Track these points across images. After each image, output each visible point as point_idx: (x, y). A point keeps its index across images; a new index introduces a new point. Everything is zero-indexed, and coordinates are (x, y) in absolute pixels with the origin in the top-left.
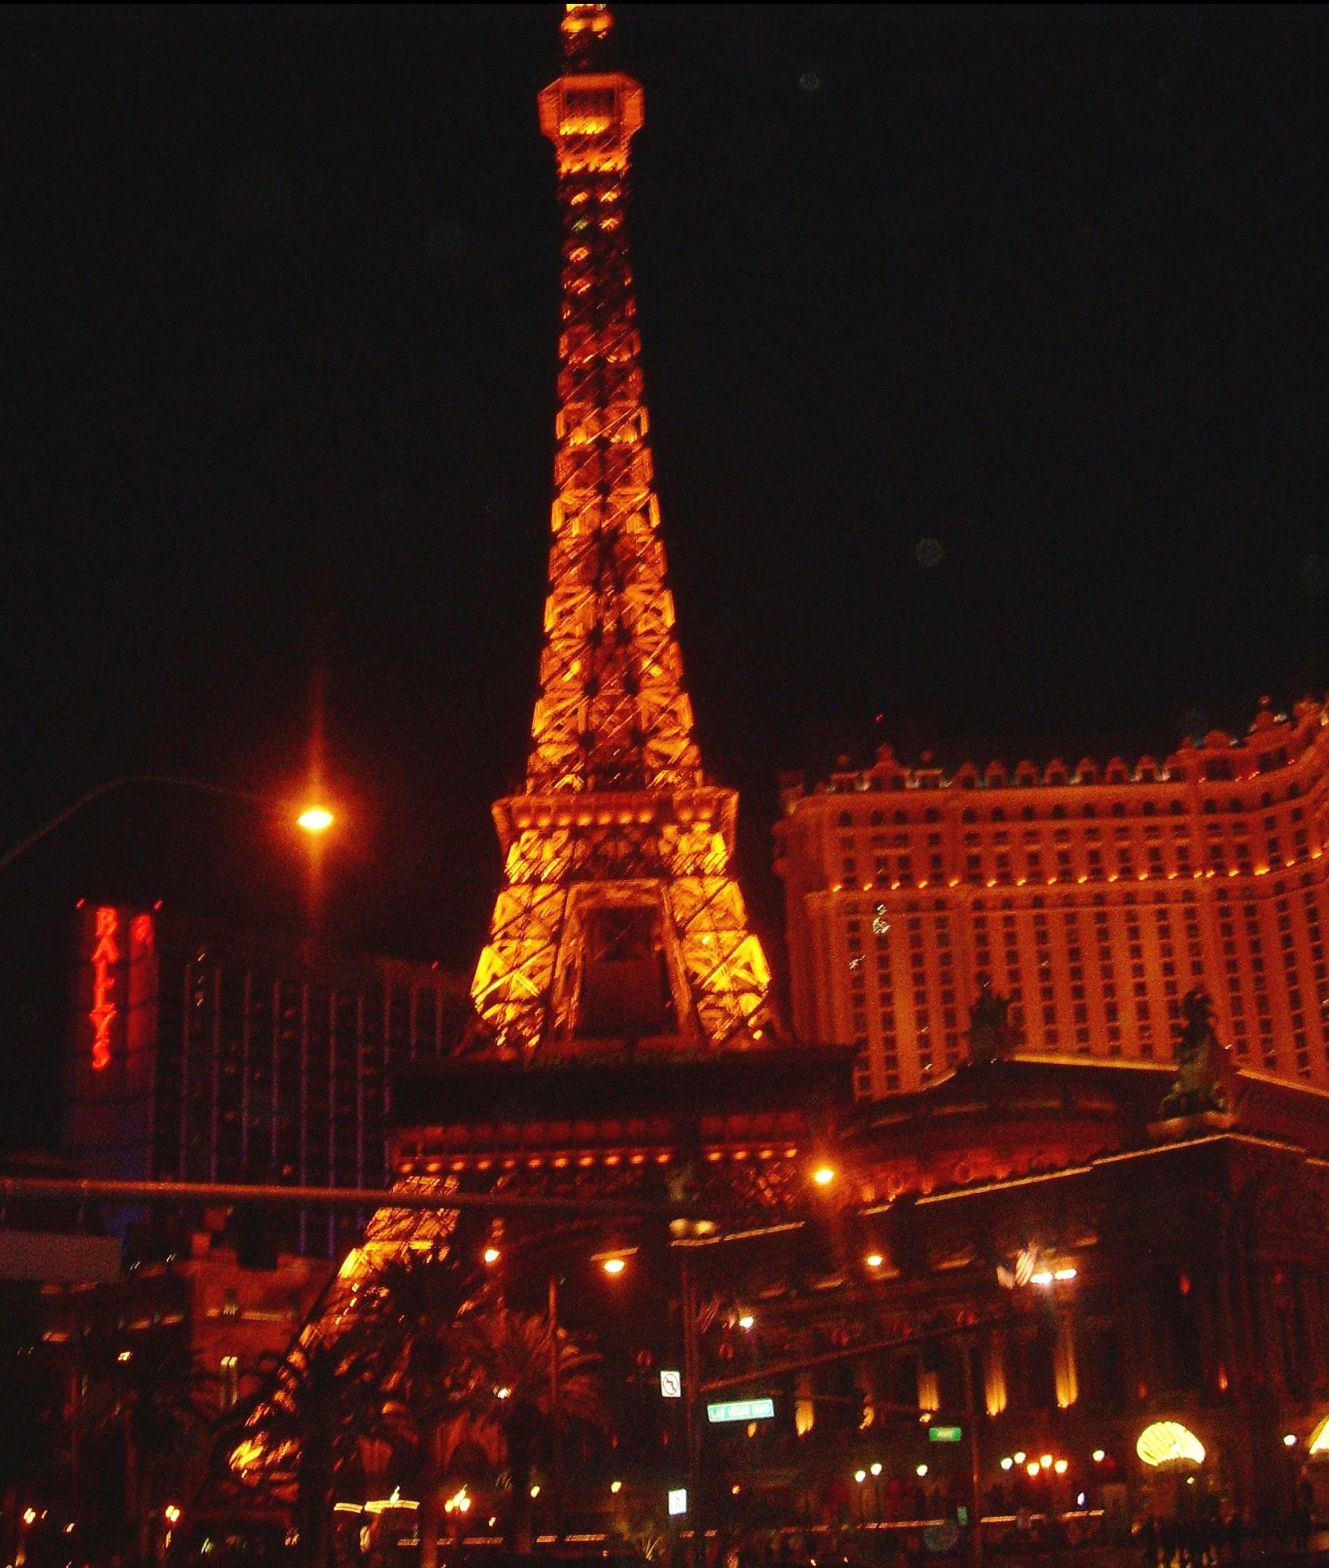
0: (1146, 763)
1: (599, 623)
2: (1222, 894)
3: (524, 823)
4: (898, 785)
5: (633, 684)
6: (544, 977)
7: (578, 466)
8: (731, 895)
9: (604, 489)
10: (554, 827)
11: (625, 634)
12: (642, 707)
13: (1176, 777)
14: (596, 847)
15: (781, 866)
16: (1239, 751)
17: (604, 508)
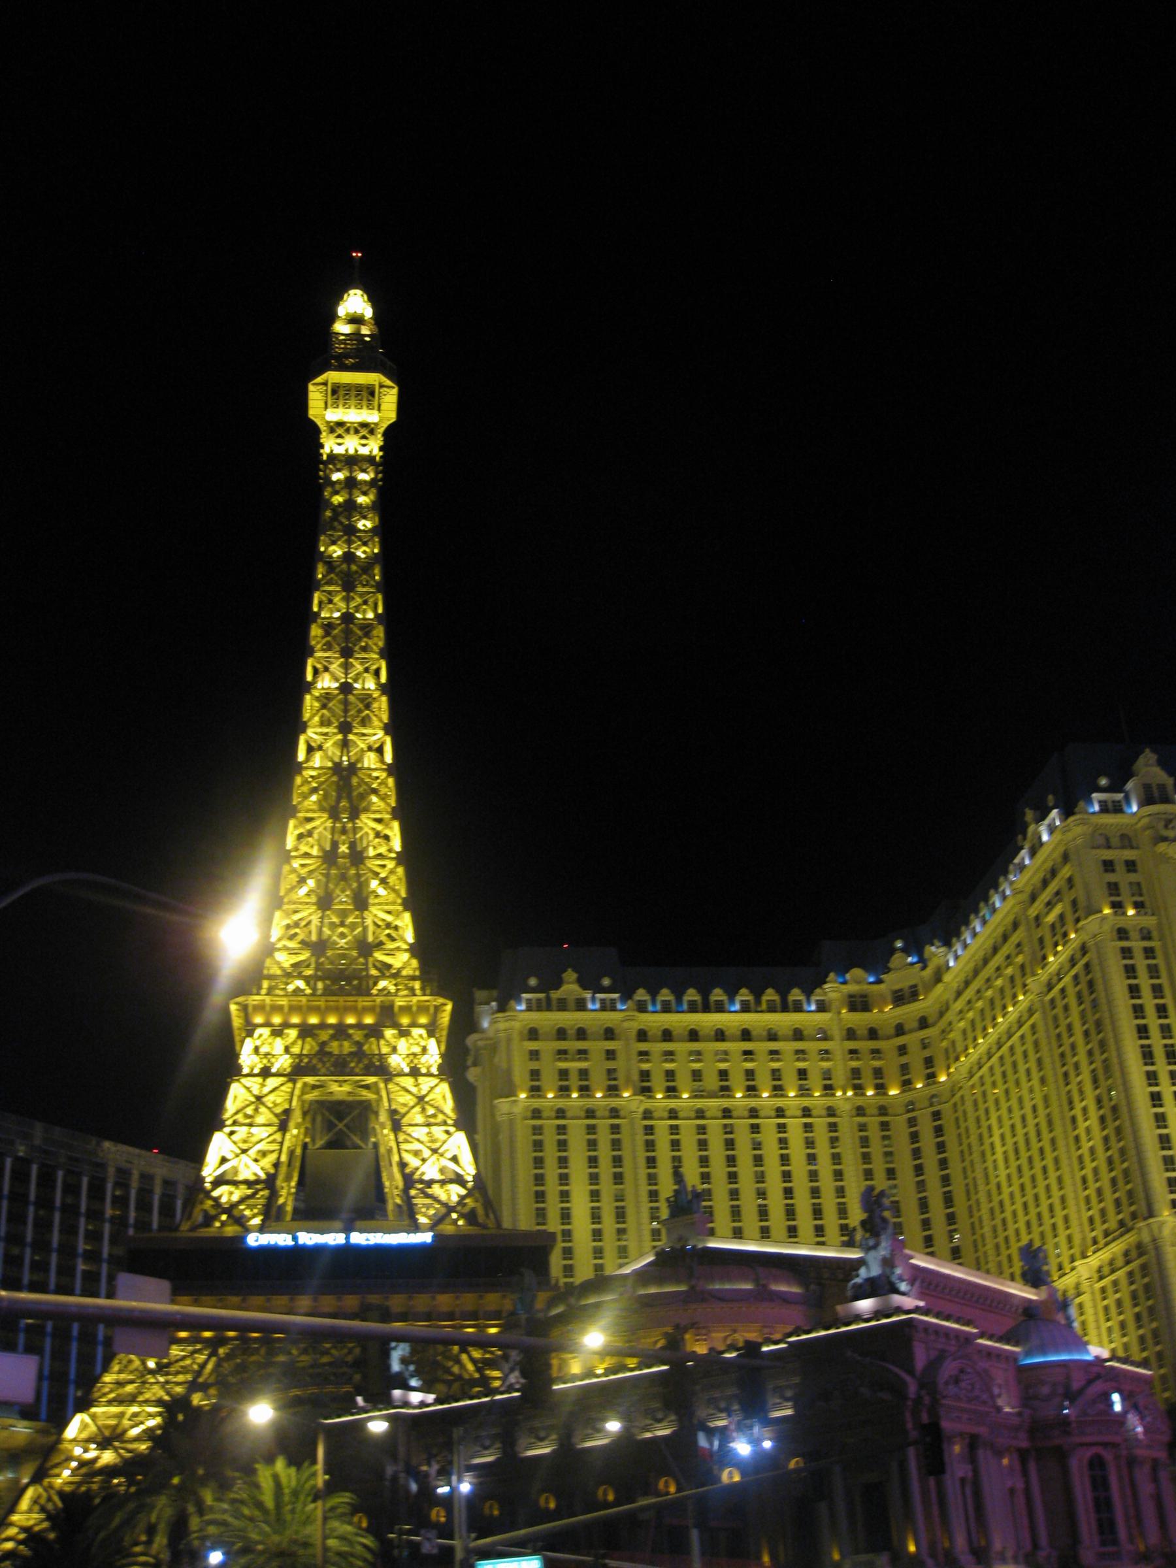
1: (335, 845)
2: (860, 1111)
3: (258, 1019)
4: (581, 1006)
5: (361, 902)
6: (267, 1162)
7: (324, 706)
8: (443, 1095)
9: (345, 728)
10: (286, 1025)
11: (357, 856)
12: (369, 922)
14: (323, 1044)
16: (876, 987)
17: (345, 745)
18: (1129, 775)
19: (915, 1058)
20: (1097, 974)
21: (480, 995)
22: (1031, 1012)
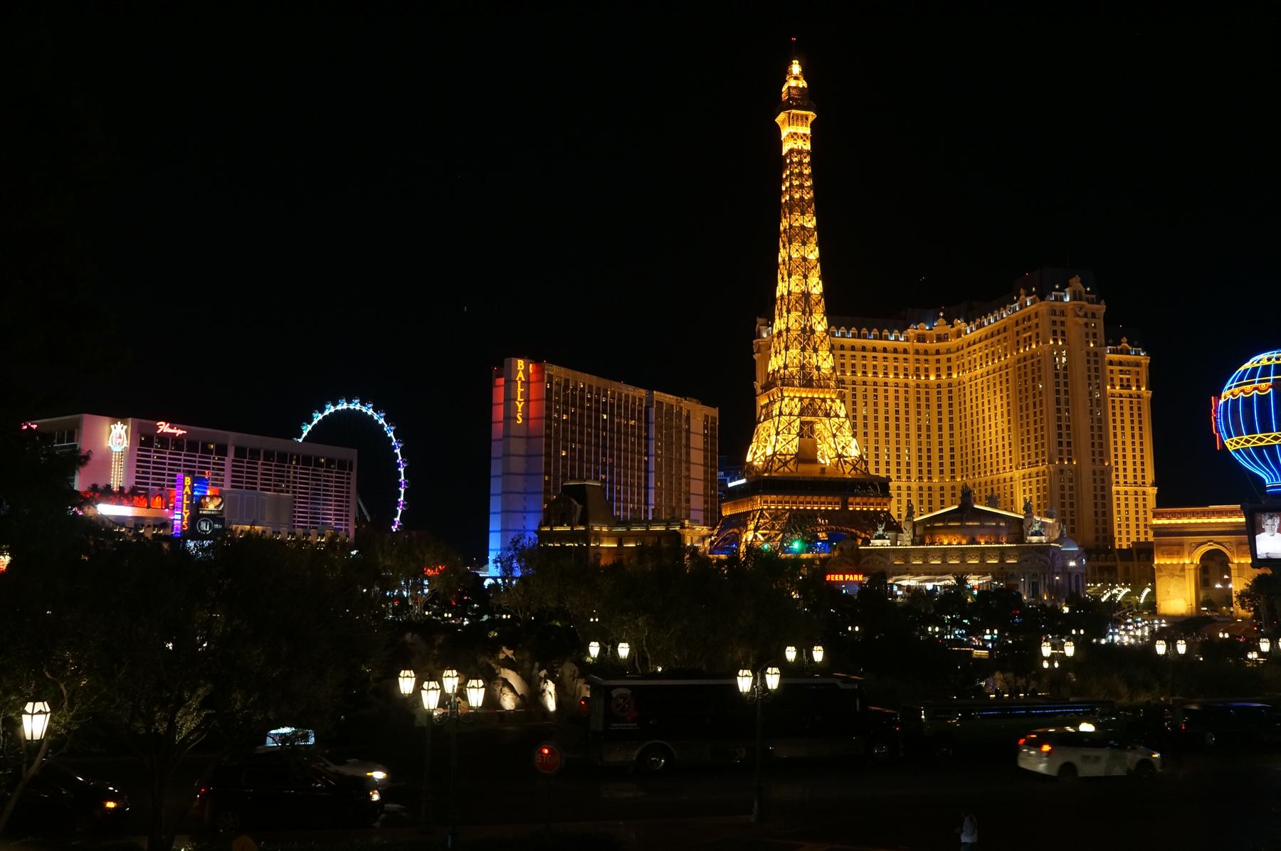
0: (896, 333)
2: (918, 386)
11: (813, 332)
13: (907, 340)
15: (756, 356)
18: (1068, 286)
19: (944, 365)
20: (1042, 365)
21: (760, 320)
22: (1007, 367)
